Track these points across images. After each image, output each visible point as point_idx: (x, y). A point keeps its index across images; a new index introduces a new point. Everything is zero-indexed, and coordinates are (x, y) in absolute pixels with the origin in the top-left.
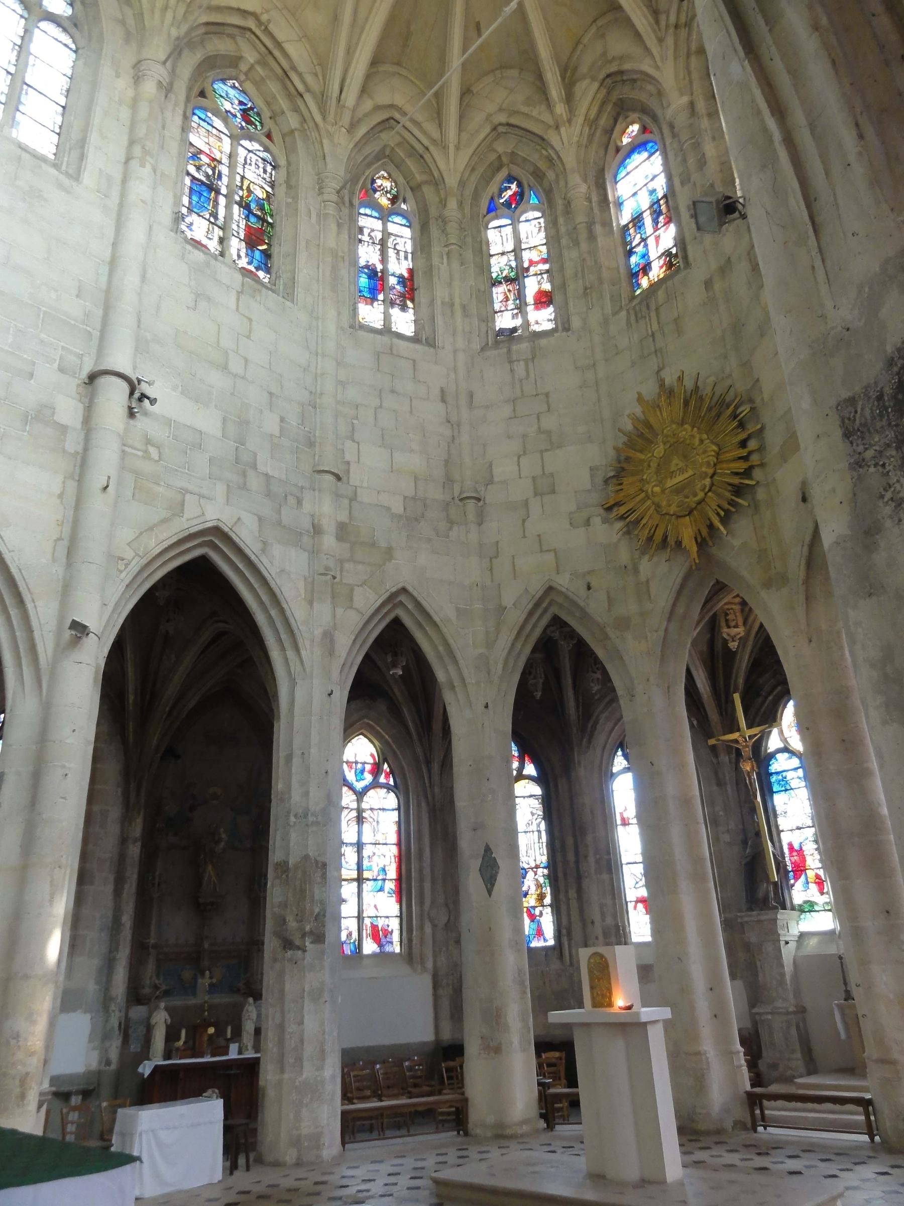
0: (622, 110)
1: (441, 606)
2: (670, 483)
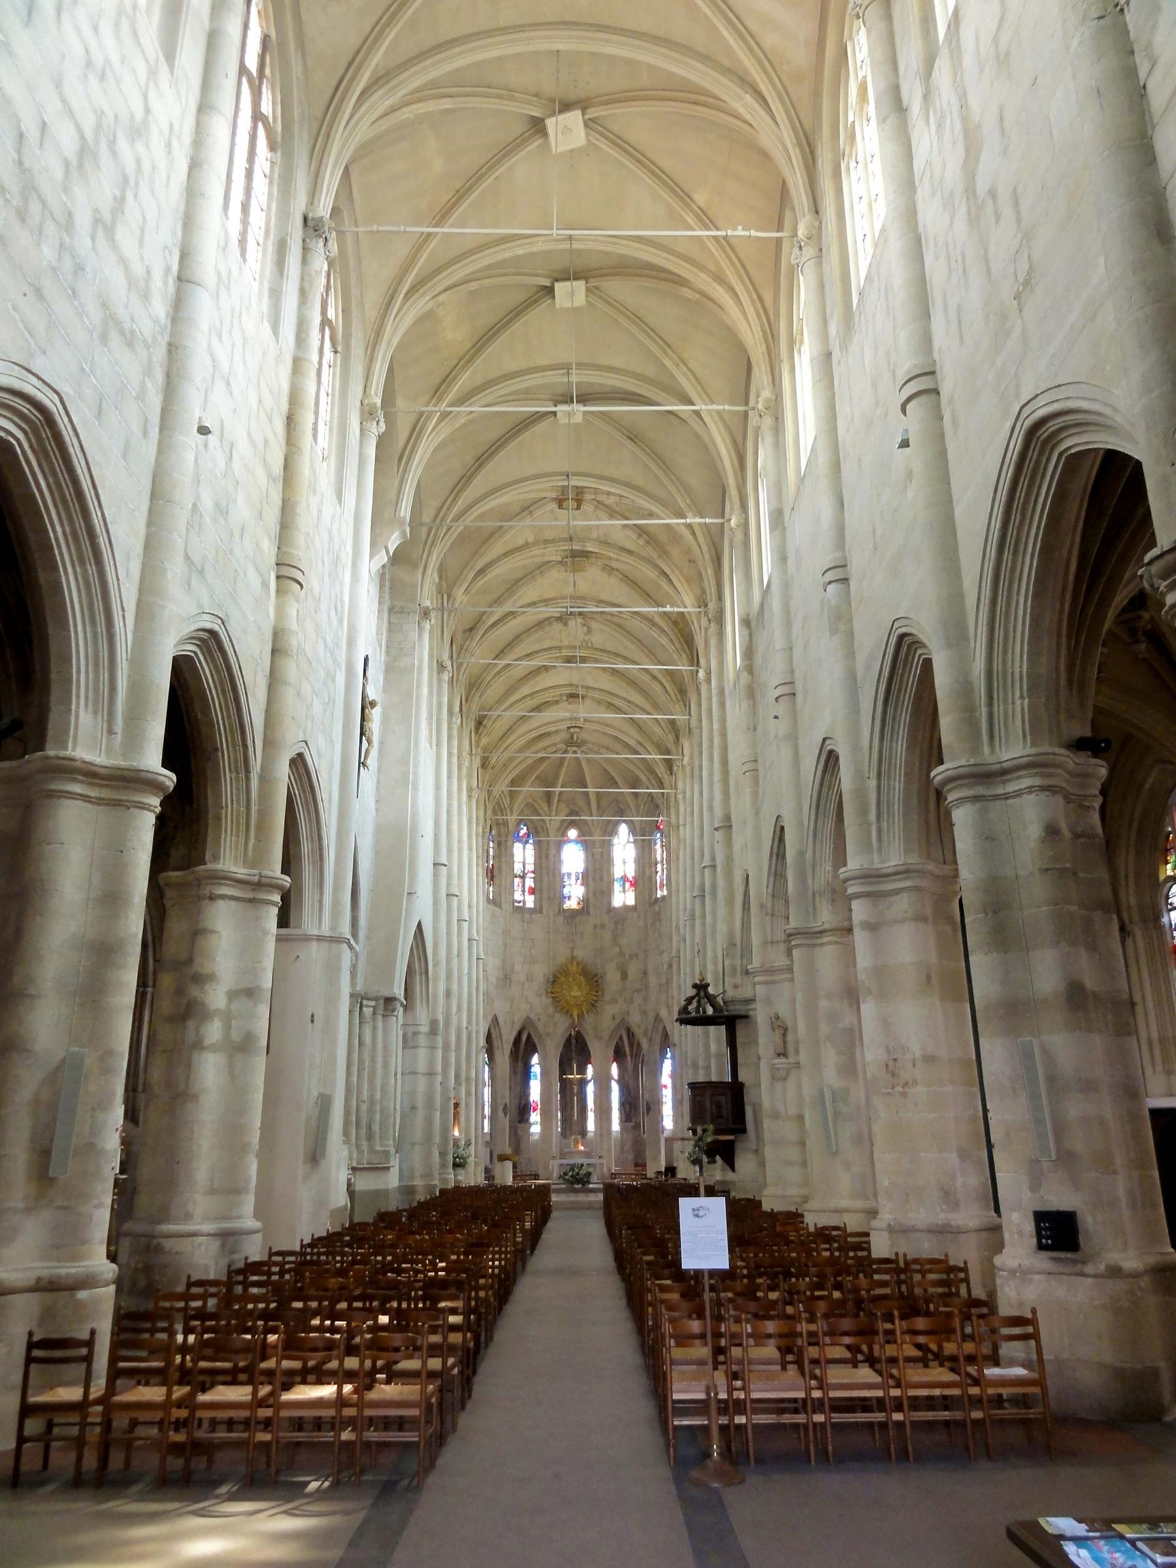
0: (573, 824)
1: (501, 1020)
2: (573, 994)
